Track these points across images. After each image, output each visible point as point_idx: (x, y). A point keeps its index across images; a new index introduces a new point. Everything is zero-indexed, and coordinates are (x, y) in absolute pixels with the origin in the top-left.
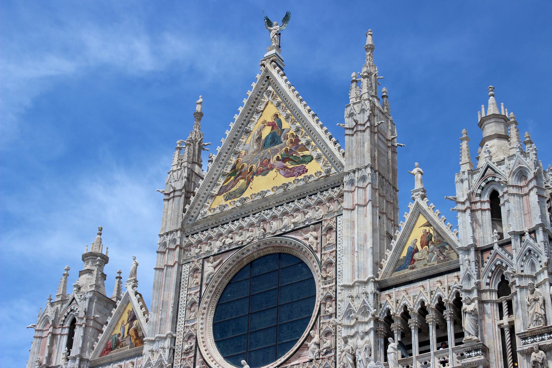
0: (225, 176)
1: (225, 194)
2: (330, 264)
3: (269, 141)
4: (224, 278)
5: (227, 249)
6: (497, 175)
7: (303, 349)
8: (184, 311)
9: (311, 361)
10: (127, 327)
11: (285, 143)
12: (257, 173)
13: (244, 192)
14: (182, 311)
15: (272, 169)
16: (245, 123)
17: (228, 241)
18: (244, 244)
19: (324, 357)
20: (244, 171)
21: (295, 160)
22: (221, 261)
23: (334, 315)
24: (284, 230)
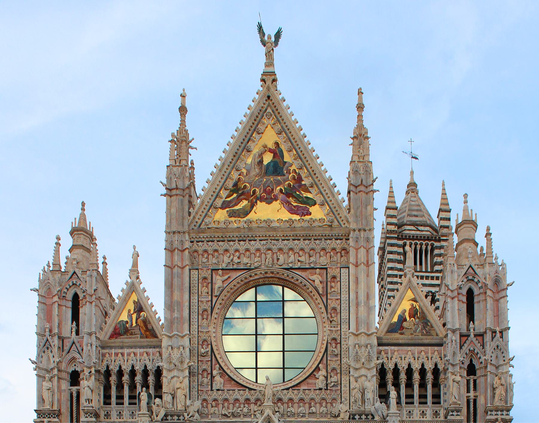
0: (228, 191)
1: (228, 209)
2: (334, 309)
3: (271, 168)
4: (232, 294)
5: (235, 267)
6: (476, 276)
7: (311, 378)
8: (196, 315)
9: (320, 389)
10: (134, 316)
11: (288, 177)
12: (261, 199)
13: (248, 214)
14: (194, 316)
15: (276, 200)
16: (247, 140)
17: (236, 260)
18: (252, 267)
19: (331, 388)
20: (246, 193)
21: (298, 198)
22: (229, 277)
23: (339, 356)
24: (291, 265)
